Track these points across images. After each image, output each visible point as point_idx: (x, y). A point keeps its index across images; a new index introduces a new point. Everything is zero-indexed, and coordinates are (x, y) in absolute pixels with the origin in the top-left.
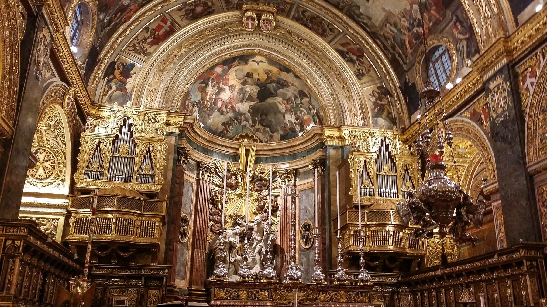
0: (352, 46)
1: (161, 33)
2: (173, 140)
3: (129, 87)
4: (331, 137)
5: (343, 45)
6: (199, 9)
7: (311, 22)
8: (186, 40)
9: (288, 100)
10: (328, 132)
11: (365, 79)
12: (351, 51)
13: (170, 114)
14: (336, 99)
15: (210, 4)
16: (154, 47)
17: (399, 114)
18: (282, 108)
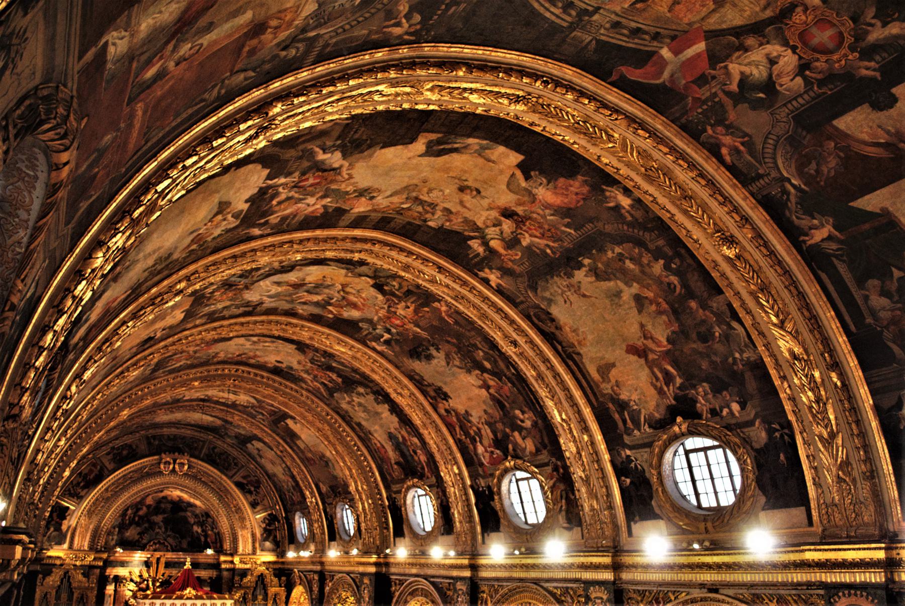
0: (252, 478)
1: (91, 477)
2: (98, 571)
3: (64, 527)
4: (225, 562)
5: (244, 477)
6: (125, 452)
7: (220, 458)
8: (113, 484)
9: (196, 516)
10: (223, 558)
11: (259, 508)
12: (250, 483)
13: (97, 551)
14: (232, 528)
15: (134, 447)
16: (85, 491)
17: (283, 538)
18: (192, 521)
